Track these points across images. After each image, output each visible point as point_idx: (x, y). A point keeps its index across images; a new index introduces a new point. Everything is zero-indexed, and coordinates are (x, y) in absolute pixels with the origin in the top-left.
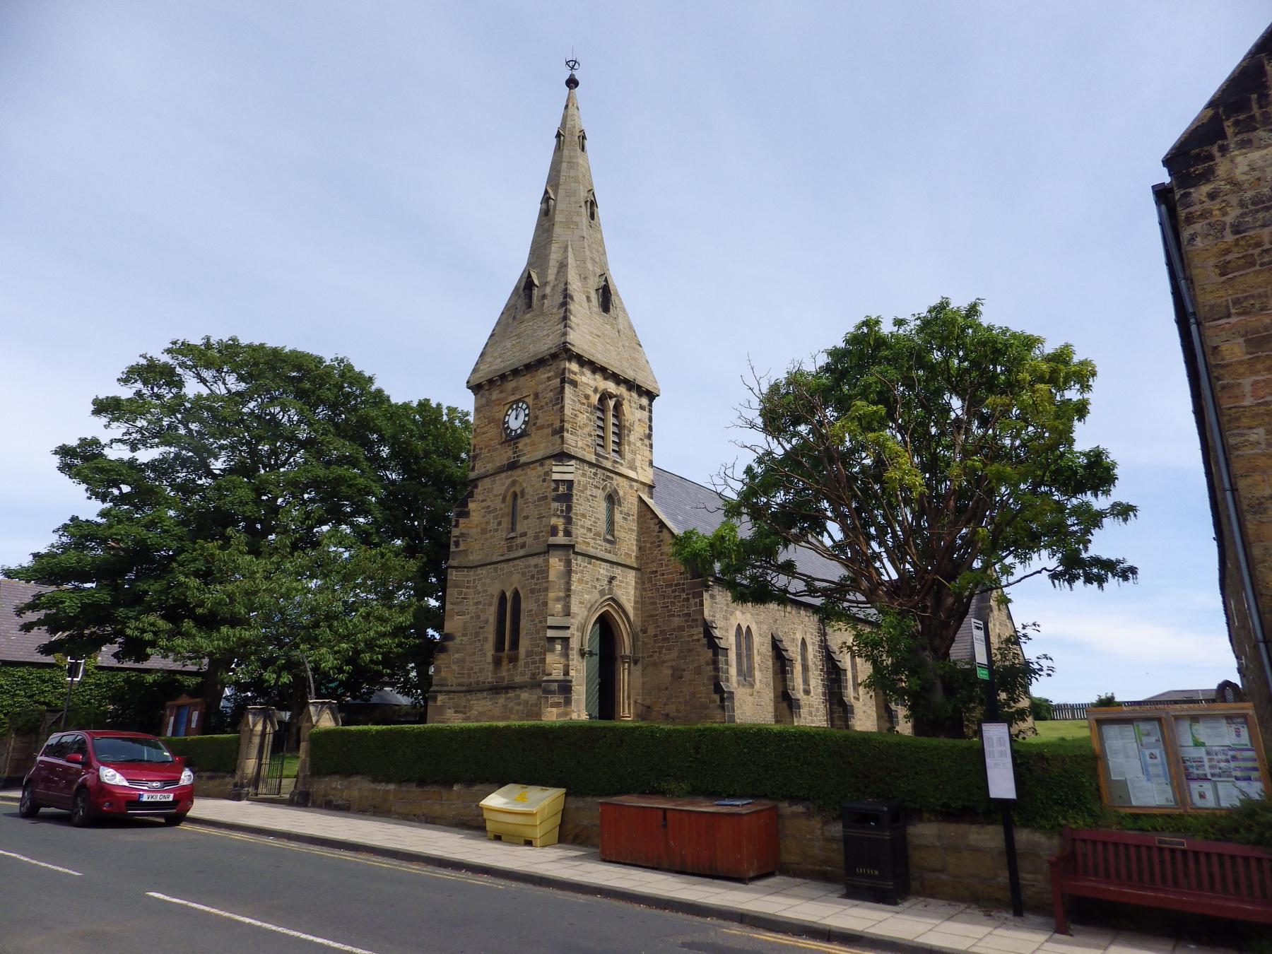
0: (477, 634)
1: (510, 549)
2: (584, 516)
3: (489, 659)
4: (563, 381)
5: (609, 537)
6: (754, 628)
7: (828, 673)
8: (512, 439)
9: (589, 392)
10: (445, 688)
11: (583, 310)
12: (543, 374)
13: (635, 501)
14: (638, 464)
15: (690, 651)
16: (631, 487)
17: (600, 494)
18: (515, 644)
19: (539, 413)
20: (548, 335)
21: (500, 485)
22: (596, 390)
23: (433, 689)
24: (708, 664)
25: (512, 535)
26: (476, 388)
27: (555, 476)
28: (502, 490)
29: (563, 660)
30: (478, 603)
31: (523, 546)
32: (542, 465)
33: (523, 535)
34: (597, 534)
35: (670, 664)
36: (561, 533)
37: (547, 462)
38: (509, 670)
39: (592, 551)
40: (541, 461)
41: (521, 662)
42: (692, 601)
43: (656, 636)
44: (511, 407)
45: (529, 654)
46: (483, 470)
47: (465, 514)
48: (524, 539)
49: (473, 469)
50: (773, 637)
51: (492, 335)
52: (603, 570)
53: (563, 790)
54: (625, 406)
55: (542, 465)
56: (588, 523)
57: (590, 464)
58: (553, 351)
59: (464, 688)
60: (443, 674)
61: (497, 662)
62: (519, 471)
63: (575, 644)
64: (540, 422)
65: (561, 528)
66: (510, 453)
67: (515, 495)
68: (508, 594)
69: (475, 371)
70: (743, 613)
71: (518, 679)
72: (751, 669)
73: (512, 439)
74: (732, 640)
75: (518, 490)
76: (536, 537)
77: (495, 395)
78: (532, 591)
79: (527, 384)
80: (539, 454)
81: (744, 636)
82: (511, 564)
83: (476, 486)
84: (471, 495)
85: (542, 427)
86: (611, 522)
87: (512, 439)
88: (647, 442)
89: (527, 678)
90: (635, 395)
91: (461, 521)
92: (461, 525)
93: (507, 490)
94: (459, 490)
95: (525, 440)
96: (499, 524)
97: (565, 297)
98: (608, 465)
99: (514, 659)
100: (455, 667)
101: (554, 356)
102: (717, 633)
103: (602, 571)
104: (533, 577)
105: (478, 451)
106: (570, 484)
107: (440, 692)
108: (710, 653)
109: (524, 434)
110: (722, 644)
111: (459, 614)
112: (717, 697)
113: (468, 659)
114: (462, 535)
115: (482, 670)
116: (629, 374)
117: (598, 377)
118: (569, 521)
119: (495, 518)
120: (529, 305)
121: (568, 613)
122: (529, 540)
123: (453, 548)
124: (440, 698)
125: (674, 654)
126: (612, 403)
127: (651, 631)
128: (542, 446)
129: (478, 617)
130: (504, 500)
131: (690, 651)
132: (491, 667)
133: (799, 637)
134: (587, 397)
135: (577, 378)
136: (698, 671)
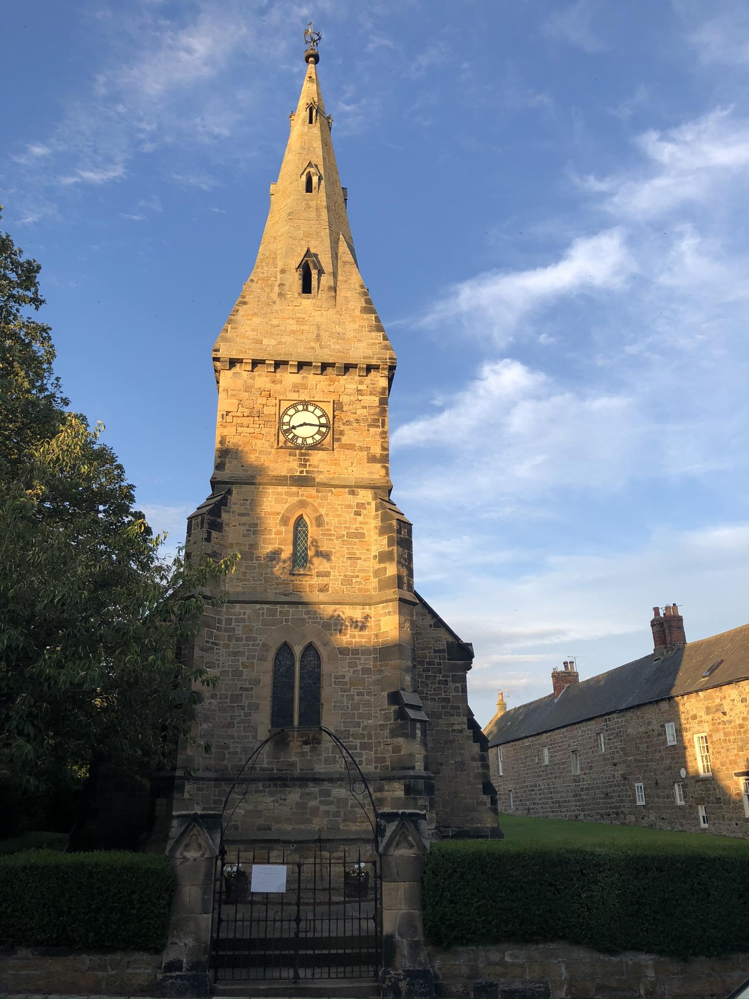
8: (299, 448)
32: (352, 493)
38: (303, 754)
44: (294, 406)
61: (279, 740)
62: (312, 491)
68: (298, 650)
71: (320, 768)
76: (347, 581)
89: (339, 767)
91: (214, 534)
93: (288, 510)
108: (476, 748)
124: (188, 787)
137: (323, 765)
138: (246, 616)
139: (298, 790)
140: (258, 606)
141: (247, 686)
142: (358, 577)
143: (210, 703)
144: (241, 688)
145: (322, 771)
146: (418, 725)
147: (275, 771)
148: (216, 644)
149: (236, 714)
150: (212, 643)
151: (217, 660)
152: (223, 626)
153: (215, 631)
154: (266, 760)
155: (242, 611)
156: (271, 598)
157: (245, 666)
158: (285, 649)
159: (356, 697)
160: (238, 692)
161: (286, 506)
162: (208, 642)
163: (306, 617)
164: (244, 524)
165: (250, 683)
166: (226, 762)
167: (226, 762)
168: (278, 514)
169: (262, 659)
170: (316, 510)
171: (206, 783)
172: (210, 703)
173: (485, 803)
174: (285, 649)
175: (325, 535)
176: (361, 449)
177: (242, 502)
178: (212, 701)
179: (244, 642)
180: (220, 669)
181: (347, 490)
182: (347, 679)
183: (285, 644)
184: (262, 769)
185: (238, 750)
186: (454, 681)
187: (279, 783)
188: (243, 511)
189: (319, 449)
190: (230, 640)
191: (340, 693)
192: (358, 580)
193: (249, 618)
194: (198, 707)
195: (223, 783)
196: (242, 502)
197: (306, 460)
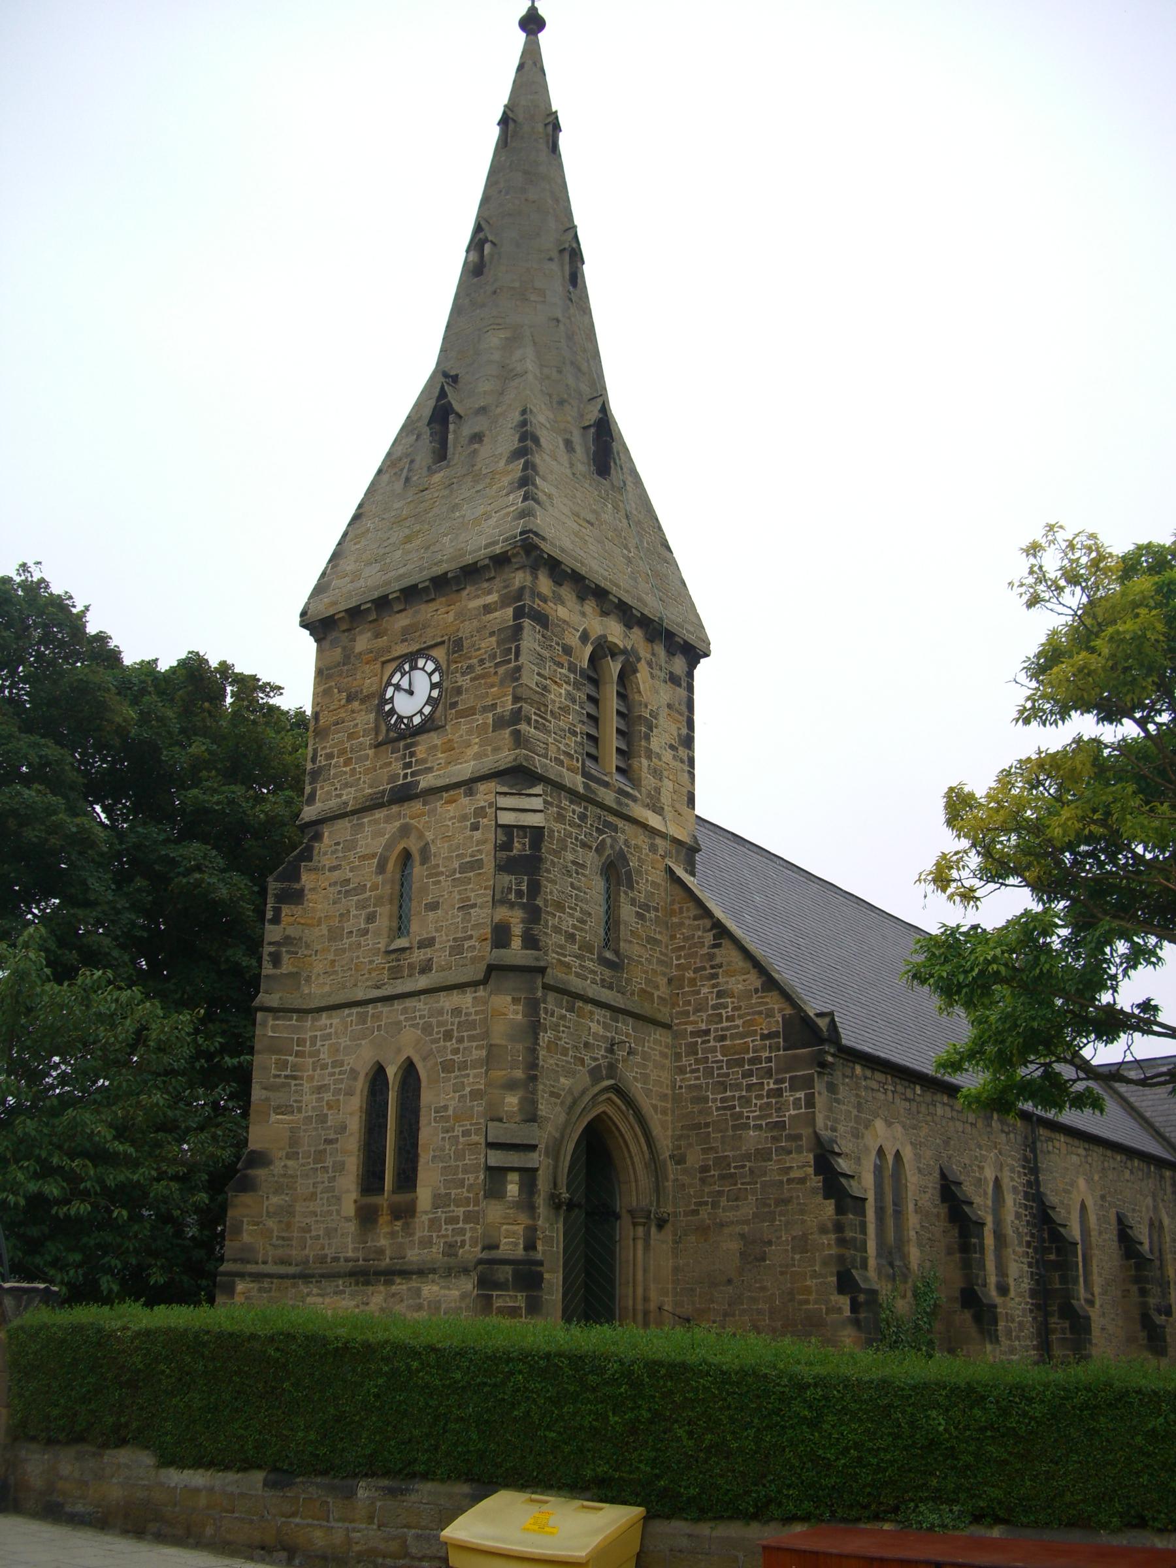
0: (320, 1155)
1: (396, 973)
2: (560, 906)
3: (349, 1209)
4: (519, 614)
5: (608, 955)
6: (908, 1154)
7: (1041, 1250)
9: (573, 640)
10: (251, 1268)
11: (557, 465)
12: (474, 600)
13: (658, 876)
14: (666, 799)
15: (786, 1202)
16: (653, 848)
17: (591, 859)
18: (407, 1179)
19: (464, 681)
20: (487, 516)
21: (375, 835)
22: (585, 637)
23: (225, 1267)
24: (823, 1230)
25: (402, 943)
26: (317, 623)
27: (506, 818)
28: (378, 846)
29: (524, 1219)
30: (320, 1089)
31: (426, 968)
32: (470, 793)
33: (428, 943)
34: (586, 947)
35: (738, 1229)
36: (516, 943)
37: (482, 787)
38: (393, 1234)
39: (576, 984)
40: (469, 785)
41: (422, 1219)
42: (789, 1097)
43: (705, 1169)
44: (399, 668)
45: (440, 1201)
46: (333, 803)
47: (296, 897)
48: (427, 953)
49: (311, 799)
50: (943, 1176)
51: (356, 518)
52: (596, 1025)
53: (637, 1511)
54: (643, 676)
55: (470, 793)
56: (568, 923)
57: (573, 794)
58: (498, 549)
59: (291, 1270)
60: (246, 1238)
61: (367, 1217)
62: (417, 806)
63: (543, 1184)
64: (466, 701)
65: (517, 930)
66: (397, 767)
67: (406, 857)
68: (391, 1071)
69: (319, 590)
70: (889, 1124)
71: (414, 1255)
72: (901, 1242)
73: (402, 737)
74: (868, 1180)
75: (414, 846)
76: (457, 949)
77: (363, 642)
78: (447, 1067)
79: (439, 616)
80: (465, 769)
81: (891, 1171)
82: (398, 1006)
83: (318, 837)
84: (307, 855)
85: (470, 712)
86: (612, 922)
87: (400, 736)
88: (683, 752)
89: (436, 1252)
90: (660, 650)
91: (286, 910)
92: (285, 920)
93: (389, 846)
94: (273, 852)
95: (435, 739)
96: (371, 918)
97: (523, 438)
98: (608, 797)
99: (405, 1213)
100: (271, 1223)
101: (501, 561)
102: (843, 1165)
103: (594, 1027)
104: (448, 1036)
105: (322, 761)
106: (537, 835)
107: (242, 1275)
108: (829, 1208)
109: (429, 725)
110: (854, 1189)
111: (279, 1110)
112: (844, 1302)
113: (299, 1207)
114: (288, 940)
115: (329, 1233)
116: (652, 605)
117: (590, 607)
118: (534, 915)
119: (361, 906)
120: (441, 454)
121: (531, 1116)
122: (440, 955)
123: (267, 969)
124: (240, 1287)
125: (747, 1209)
126: (614, 667)
127: (694, 1158)
128: (471, 752)
129: (323, 1119)
130: (381, 868)
131: (786, 1202)
132: (352, 1227)
133: (989, 1174)
134: (567, 650)
135: (550, 608)
136: (802, 1244)
137: (416, 1251)
138: (333, 1030)
139: (382, 1288)
140: (347, 1011)
141: (332, 1136)
142: (471, 937)
143: (285, 1166)
144: (325, 1140)
145: (415, 1259)
146: (514, 1177)
147: (361, 1262)
148: (294, 1078)
149: (319, 1180)
150: (286, 1077)
151: (296, 1101)
152: (307, 1049)
153: (290, 1058)
154: (351, 1246)
155: (328, 1022)
156: (360, 995)
157: (330, 1107)
158: (379, 1072)
159: (461, 1139)
160: (322, 1147)
161: (383, 840)
162: (279, 1076)
163: (402, 1018)
164: (335, 884)
165: (335, 1132)
166: (307, 1252)
167: (307, 1252)
168: (374, 856)
169: (350, 1093)
170: (421, 836)
171: (275, 1281)
172: (285, 1166)
173: (840, 1310)
174: (379, 1072)
175: (430, 876)
176: (485, 709)
177: (334, 848)
178: (290, 1163)
179: (330, 1070)
180: (303, 1114)
181: (462, 790)
182: (450, 1112)
183: (378, 1062)
184: (347, 1260)
185: (321, 1233)
186: (793, 1089)
187: (362, 1279)
188: (335, 863)
189: (429, 731)
190: (314, 1070)
191: (441, 1135)
192: (472, 943)
193: (336, 1033)
194: (260, 1173)
195: (300, 1282)
196: (334, 848)
197: (412, 755)
